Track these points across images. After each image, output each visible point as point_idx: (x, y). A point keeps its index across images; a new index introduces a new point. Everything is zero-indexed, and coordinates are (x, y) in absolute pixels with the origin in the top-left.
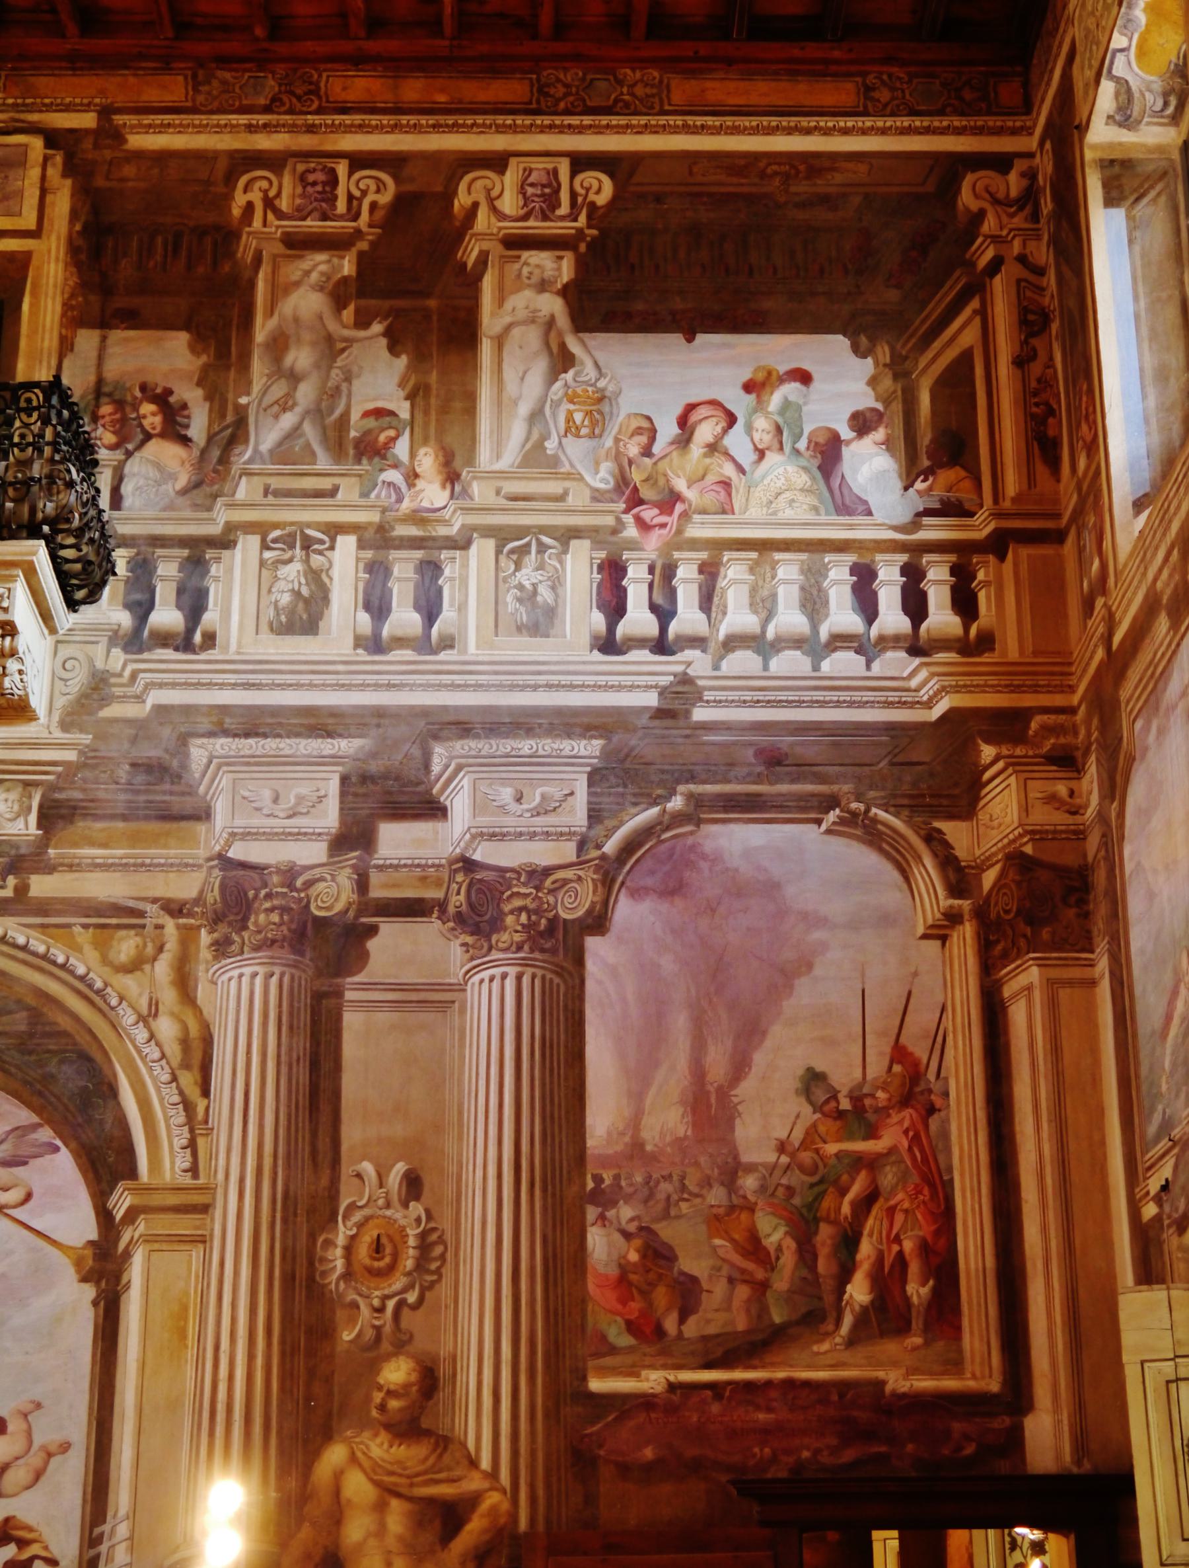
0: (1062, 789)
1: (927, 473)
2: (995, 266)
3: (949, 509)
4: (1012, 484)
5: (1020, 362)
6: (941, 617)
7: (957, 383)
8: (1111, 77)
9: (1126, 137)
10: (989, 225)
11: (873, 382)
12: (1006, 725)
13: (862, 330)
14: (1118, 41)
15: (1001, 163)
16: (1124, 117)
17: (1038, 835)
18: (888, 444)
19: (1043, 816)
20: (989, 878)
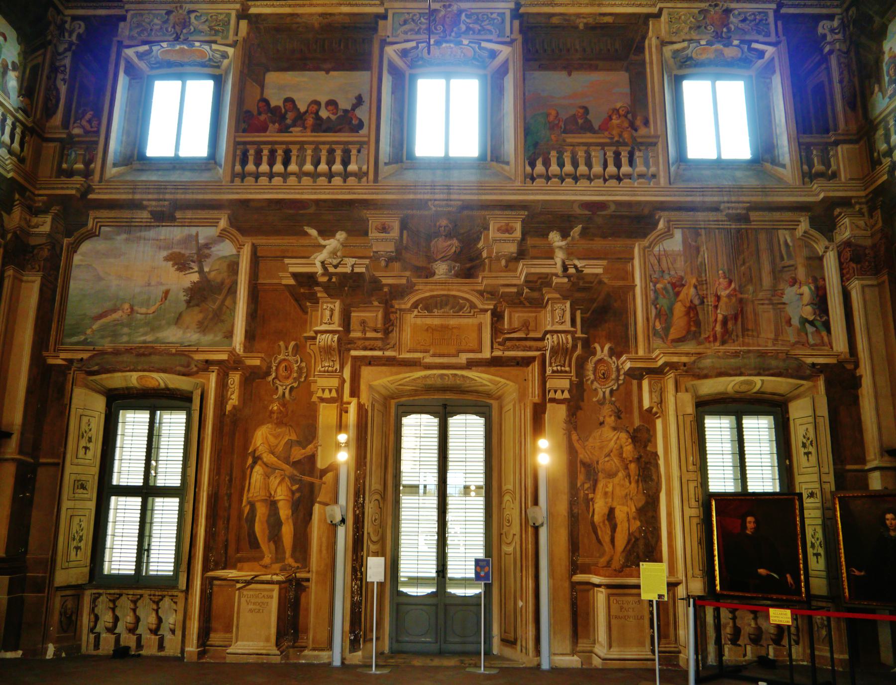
0: (28, 217)
1: (24, 96)
2: (50, 42)
3: (24, 111)
4: (38, 116)
5: (48, 78)
6: (16, 146)
7: (35, 70)
8: (151, 48)
9: (136, 60)
10: (52, 28)
11: (19, 54)
12: (22, 190)
13: (23, 38)
14: (164, 45)
15: (59, 12)
16: (140, 56)
17: (22, 229)
18: (17, 77)
19: (23, 224)
20: (9, 236)
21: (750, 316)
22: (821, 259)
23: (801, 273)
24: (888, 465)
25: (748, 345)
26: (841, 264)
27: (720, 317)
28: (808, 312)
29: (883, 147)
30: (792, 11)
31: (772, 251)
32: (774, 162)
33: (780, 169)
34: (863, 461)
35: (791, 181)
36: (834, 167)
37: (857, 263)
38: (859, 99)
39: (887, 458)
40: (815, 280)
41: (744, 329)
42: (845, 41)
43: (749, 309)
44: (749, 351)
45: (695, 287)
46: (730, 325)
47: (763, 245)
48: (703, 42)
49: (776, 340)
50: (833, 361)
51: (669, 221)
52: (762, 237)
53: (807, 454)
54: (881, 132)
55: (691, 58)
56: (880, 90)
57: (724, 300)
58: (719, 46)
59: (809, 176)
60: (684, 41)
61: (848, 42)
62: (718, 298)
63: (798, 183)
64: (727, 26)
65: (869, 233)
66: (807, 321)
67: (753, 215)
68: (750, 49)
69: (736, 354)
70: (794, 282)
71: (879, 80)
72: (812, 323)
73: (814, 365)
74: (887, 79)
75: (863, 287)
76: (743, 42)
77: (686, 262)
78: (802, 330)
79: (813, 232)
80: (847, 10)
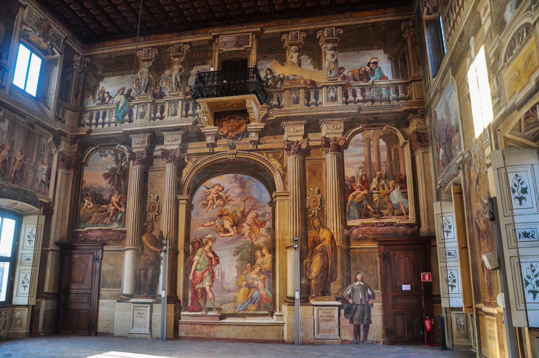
21: (25, 173)
22: (53, 155)
23: (46, 159)
24: (55, 249)
25: (22, 186)
26: (58, 160)
27: (14, 169)
28: (44, 177)
29: (88, 121)
30: (69, 43)
31: (39, 145)
32: (46, 104)
33: (47, 109)
34: (48, 247)
35: (51, 117)
36: (65, 118)
37: (63, 162)
38: (80, 95)
39: (55, 246)
40: (49, 165)
41: (22, 179)
42: (80, 68)
43: (26, 169)
44: (21, 189)
45: (8, 151)
46: (17, 174)
47: (36, 142)
48: (37, 34)
49: (31, 187)
50: (47, 201)
51: (5, 114)
52: (37, 137)
53: (30, 241)
54: (88, 115)
55: (28, 36)
56: (93, 98)
57: (18, 162)
58: (41, 39)
59: (57, 118)
60: (31, 28)
61: (81, 70)
62: (16, 160)
63: (53, 119)
64: (48, 33)
65: (68, 151)
66: (43, 181)
67: (36, 126)
68: (51, 49)
69: (16, 189)
70: (43, 163)
71: (94, 95)
72: (44, 183)
73: (41, 202)
74: (97, 96)
75: (62, 173)
76: (51, 44)
77: (7, 137)
78: (41, 185)
79: (53, 143)
80: (86, 57)
